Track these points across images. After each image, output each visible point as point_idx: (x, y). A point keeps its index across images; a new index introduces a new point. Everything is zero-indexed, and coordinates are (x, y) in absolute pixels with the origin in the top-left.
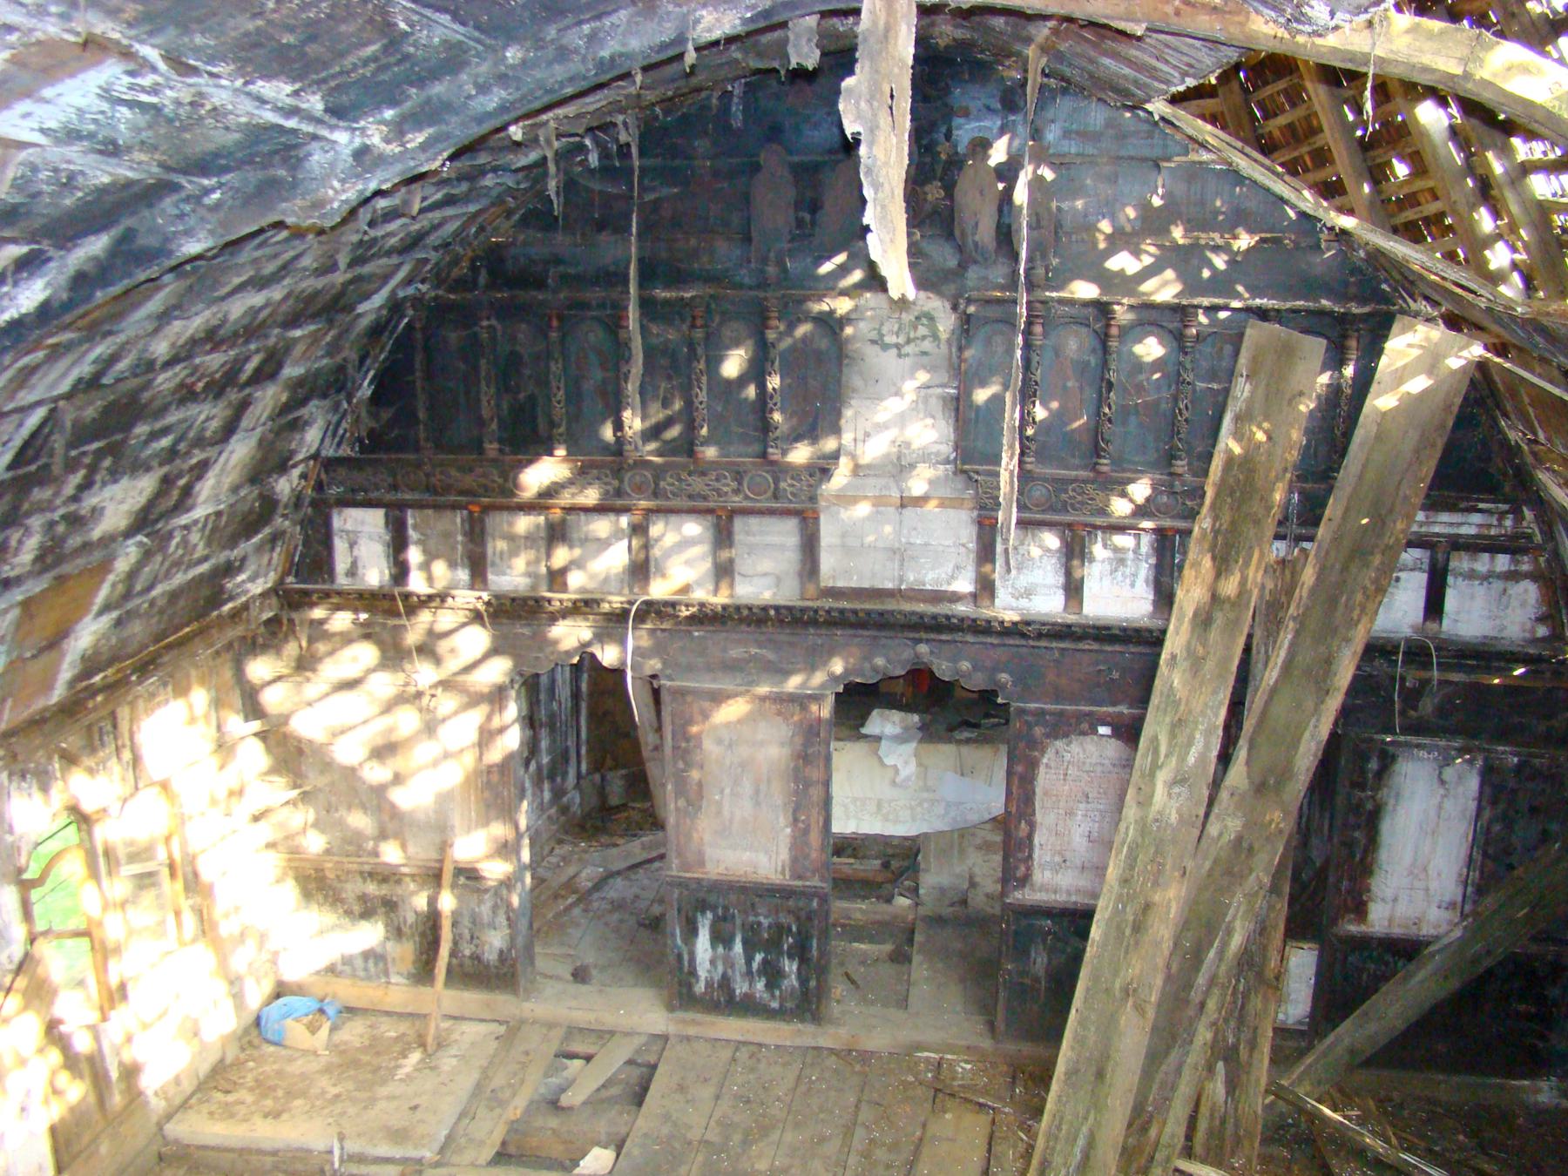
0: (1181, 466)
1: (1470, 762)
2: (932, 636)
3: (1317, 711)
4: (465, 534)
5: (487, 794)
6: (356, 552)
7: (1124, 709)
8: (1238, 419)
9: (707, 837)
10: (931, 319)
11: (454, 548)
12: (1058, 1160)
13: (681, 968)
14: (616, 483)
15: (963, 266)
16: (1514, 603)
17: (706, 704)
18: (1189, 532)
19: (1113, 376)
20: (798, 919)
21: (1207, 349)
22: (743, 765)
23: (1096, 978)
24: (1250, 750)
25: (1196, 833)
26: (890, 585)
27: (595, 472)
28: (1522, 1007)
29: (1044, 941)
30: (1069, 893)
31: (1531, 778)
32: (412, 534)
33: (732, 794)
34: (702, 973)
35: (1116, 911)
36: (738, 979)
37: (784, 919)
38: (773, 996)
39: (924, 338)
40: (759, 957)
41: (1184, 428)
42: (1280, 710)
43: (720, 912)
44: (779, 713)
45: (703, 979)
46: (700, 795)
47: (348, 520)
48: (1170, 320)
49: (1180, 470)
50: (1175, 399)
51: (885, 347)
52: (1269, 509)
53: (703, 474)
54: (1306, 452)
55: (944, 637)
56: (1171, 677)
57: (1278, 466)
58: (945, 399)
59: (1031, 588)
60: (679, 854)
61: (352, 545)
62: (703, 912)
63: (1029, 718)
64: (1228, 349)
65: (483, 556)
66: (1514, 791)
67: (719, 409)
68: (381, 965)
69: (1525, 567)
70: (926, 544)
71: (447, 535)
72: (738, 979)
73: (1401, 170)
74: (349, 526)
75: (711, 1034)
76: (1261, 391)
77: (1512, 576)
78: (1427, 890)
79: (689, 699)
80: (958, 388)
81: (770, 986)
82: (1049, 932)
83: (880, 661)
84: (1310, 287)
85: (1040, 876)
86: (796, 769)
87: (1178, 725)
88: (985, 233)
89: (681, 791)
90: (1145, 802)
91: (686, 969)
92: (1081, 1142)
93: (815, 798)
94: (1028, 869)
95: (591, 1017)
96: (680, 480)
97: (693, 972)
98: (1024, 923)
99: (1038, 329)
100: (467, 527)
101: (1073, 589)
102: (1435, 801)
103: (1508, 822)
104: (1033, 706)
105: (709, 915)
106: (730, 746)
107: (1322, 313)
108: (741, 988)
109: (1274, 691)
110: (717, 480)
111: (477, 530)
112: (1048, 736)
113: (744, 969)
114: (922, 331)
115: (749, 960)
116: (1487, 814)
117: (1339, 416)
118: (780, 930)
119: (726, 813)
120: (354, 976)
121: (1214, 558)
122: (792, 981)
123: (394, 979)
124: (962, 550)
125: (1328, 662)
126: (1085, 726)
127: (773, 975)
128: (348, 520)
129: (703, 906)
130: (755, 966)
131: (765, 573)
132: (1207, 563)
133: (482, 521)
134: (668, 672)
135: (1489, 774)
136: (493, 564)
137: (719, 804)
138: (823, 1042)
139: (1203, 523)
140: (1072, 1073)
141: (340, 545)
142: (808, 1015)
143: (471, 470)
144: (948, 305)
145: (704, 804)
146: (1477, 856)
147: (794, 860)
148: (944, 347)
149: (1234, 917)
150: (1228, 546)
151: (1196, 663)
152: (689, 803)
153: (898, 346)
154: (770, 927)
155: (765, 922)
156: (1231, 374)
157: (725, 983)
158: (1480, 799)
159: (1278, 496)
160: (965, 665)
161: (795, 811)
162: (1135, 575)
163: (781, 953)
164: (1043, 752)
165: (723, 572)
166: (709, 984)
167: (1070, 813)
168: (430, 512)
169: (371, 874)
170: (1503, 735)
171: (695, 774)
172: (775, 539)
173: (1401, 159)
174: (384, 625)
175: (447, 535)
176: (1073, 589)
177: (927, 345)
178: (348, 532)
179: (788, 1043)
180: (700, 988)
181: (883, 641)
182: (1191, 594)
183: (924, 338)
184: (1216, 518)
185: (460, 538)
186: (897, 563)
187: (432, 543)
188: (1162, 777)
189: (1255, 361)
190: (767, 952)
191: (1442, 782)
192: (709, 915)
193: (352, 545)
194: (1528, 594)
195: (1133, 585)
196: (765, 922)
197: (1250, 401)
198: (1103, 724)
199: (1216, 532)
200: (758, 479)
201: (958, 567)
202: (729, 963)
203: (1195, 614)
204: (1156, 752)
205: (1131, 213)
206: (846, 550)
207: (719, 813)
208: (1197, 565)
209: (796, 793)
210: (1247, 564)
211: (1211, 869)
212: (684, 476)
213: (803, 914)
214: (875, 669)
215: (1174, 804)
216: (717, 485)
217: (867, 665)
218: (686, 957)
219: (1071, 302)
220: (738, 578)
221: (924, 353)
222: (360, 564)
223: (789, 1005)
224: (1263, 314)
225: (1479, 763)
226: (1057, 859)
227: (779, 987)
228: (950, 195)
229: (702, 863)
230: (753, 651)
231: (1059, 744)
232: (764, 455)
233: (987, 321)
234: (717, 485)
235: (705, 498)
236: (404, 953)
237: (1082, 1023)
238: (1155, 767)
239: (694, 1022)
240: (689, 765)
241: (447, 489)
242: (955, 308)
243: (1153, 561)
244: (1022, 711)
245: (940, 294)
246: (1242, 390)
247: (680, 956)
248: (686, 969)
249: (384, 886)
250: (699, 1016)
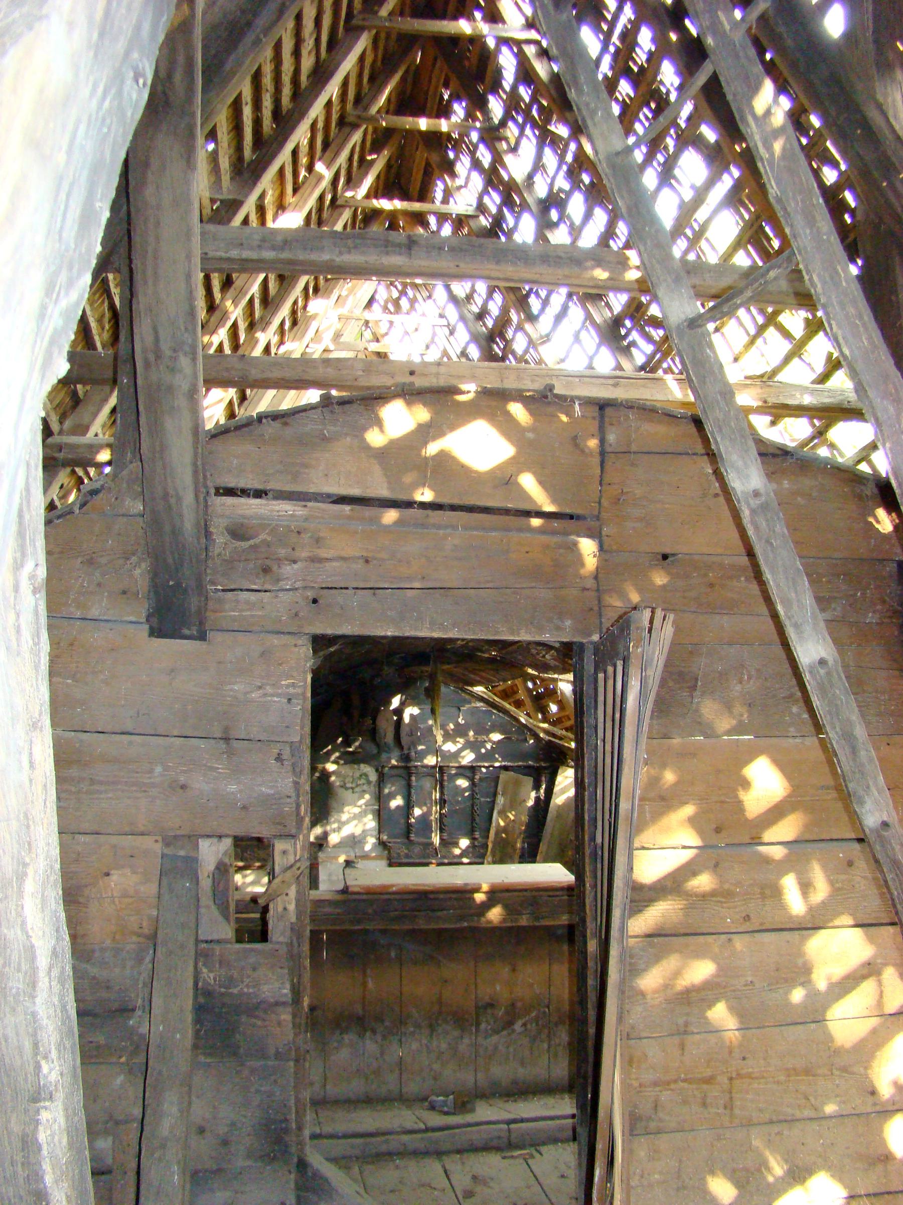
0: (477, 835)
8: (499, 813)
10: (366, 775)
15: (379, 753)
19: (446, 797)
21: (484, 784)
41: (477, 819)
48: (470, 771)
50: (473, 805)
51: (347, 789)
52: (515, 850)
54: (528, 825)
57: (517, 832)
64: (493, 784)
73: (554, 708)
76: (508, 801)
84: (524, 756)
88: (390, 738)
99: (413, 778)
107: (529, 767)
117: (542, 807)
148: (372, 788)
156: (495, 795)
159: (519, 845)
173: (554, 703)
189: (504, 788)
197: (504, 805)
205: (452, 726)
219: (427, 766)
224: (506, 768)
228: (374, 722)
233: (392, 776)
242: (377, 770)
245: (370, 765)
246: (500, 800)
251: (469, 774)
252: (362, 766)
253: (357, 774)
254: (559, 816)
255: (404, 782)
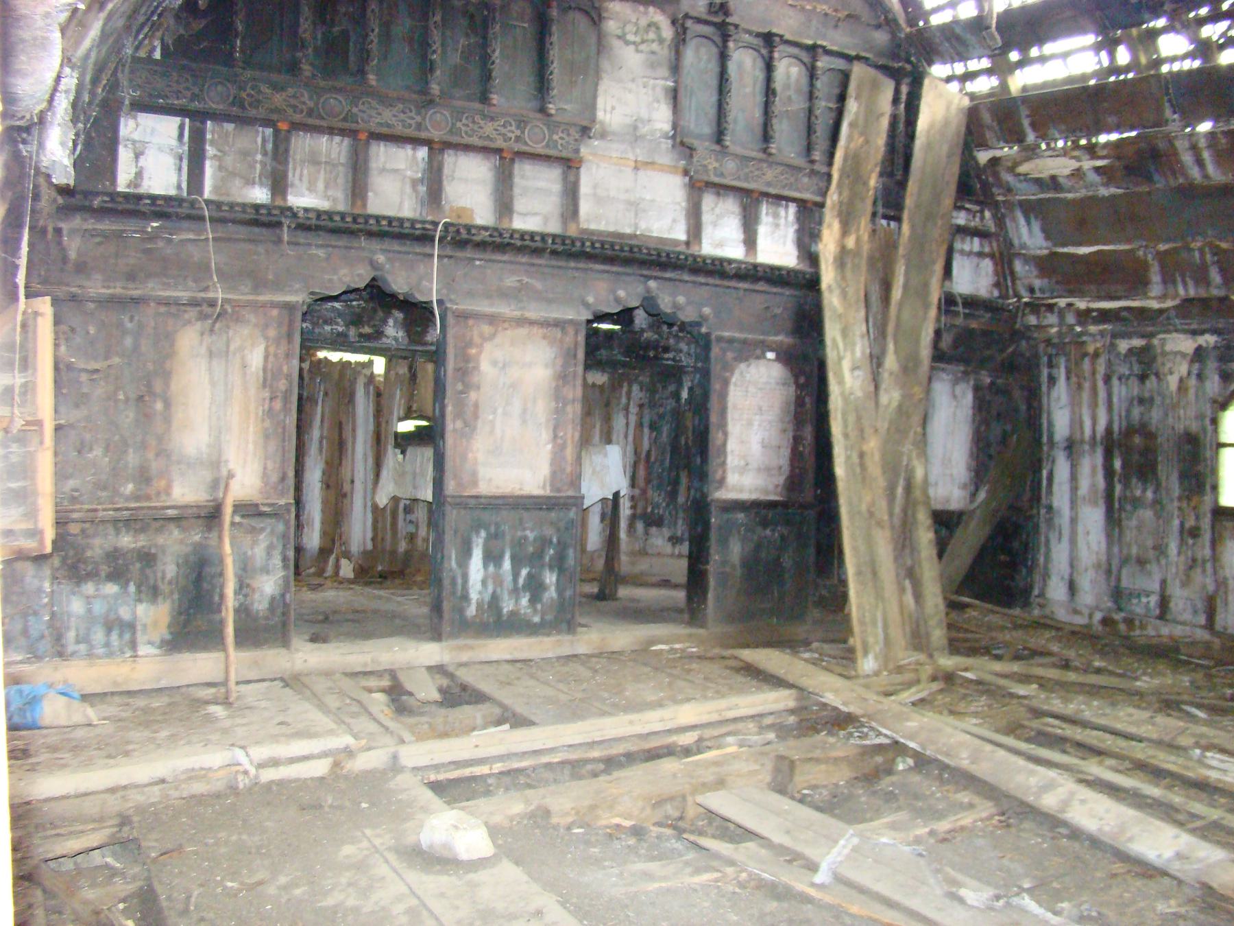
1: (968, 382)
2: (659, 274)
3: (925, 318)
4: (265, 154)
5: (267, 423)
6: (142, 162)
7: (780, 338)
8: (851, 125)
9: (481, 457)
10: (658, 28)
11: (252, 167)
12: (871, 640)
13: (454, 593)
14: (419, 119)
16: (983, 273)
17: (486, 329)
18: (821, 205)
20: (558, 530)
22: (513, 386)
23: (850, 504)
24: (896, 343)
25: (873, 405)
26: (628, 231)
27: (401, 106)
28: (1002, 557)
29: (739, 532)
30: (750, 492)
31: (996, 393)
32: (210, 150)
33: (505, 414)
34: (474, 596)
35: (848, 458)
36: (506, 596)
37: (549, 532)
38: (535, 610)
39: (653, 41)
40: (524, 572)
42: (906, 315)
43: (493, 529)
44: (544, 337)
45: (474, 602)
46: (476, 416)
47: (134, 127)
49: (817, 158)
51: (627, 43)
53: (492, 119)
55: (668, 275)
56: (832, 300)
58: (666, 90)
59: (723, 238)
60: (455, 477)
61: (138, 155)
62: (478, 533)
63: (724, 345)
65: (284, 176)
66: (989, 402)
67: (506, 68)
68: (127, 636)
69: (987, 250)
70: (653, 201)
71: (245, 154)
72: (506, 596)
74: (136, 136)
75: (483, 656)
76: (862, 109)
77: (981, 255)
78: (951, 475)
79: (471, 322)
80: (675, 82)
81: (534, 600)
82: (742, 525)
83: (621, 293)
85: (732, 478)
86: (557, 389)
87: (845, 332)
89: (459, 415)
90: (841, 382)
91: (459, 594)
92: (880, 624)
93: (570, 416)
94: (724, 472)
95: (367, 658)
96: (474, 122)
97: (465, 597)
98: (726, 516)
100: (270, 146)
101: (750, 242)
102: (952, 410)
103: (988, 425)
104: (726, 334)
105: (483, 534)
106: (504, 366)
108: (508, 606)
109: (901, 304)
110: (504, 126)
111: (281, 149)
112: (735, 359)
113: (511, 586)
114: (652, 36)
115: (516, 575)
116: (978, 418)
118: (544, 542)
119: (498, 431)
120: (90, 655)
121: (841, 222)
122: (551, 593)
123: (143, 650)
124: (678, 207)
125: (926, 285)
126: (758, 352)
127: (535, 587)
128: (134, 127)
129: (477, 526)
130: (521, 581)
131: (536, 211)
132: (836, 225)
133: (287, 140)
134: (453, 297)
135: (977, 389)
136: (292, 185)
137: (492, 423)
138: (582, 649)
139: (833, 198)
140: (859, 573)
141: (124, 154)
142: (564, 626)
143: (283, 89)
144: (669, 22)
145: (480, 424)
146: (975, 450)
147: (554, 474)
149: (910, 460)
150: (849, 214)
151: (844, 294)
152: (466, 424)
153: (634, 43)
154: (535, 540)
155: (531, 535)
157: (495, 600)
158: (973, 408)
160: (681, 299)
161: (556, 428)
162: (785, 236)
163: (543, 566)
164: (732, 374)
165: (504, 205)
166: (480, 605)
167: (750, 423)
168: (230, 127)
169: (127, 522)
170: (982, 363)
171: (473, 395)
172: (541, 184)
174: (170, 241)
175: (245, 154)
176: (750, 242)
177: (655, 46)
178: (134, 142)
179: (550, 655)
180: (471, 611)
181: (624, 278)
182: (828, 244)
183: (653, 41)
184: (840, 194)
185: (259, 157)
186: (632, 214)
187: (229, 160)
188: (846, 365)
189: (859, 87)
190: (532, 567)
191: (954, 396)
192: (483, 534)
193: (138, 155)
194: (987, 265)
195: (784, 244)
196: (531, 535)
197: (857, 114)
198: (772, 350)
199: (841, 203)
200: (537, 130)
201: (674, 221)
202: (498, 581)
203: (835, 259)
204: (838, 348)
206: (599, 200)
207: (492, 432)
208: (830, 226)
209: (557, 411)
210: (858, 229)
211: (888, 429)
212: (477, 118)
213: (562, 525)
214: (618, 300)
215: (858, 383)
216: (503, 130)
217: (611, 298)
218: (460, 581)
220: (515, 216)
221: (653, 53)
222: (146, 175)
223: (549, 617)
225: (972, 383)
226: (743, 463)
227: (540, 600)
229: (475, 483)
230: (526, 280)
231: (743, 366)
232: (543, 110)
234: (503, 130)
235: (491, 140)
236: (154, 616)
237: (853, 537)
238: (840, 359)
239: (471, 648)
240: (468, 387)
241: (256, 103)
242: (674, 22)
243: (796, 227)
244: (720, 339)
245: (663, 11)
247: (454, 580)
248: (459, 594)
249: (142, 537)
250: (470, 642)
251: (806, 59)
252: (651, 9)
253: (643, 22)
254: (929, 146)
255: (715, 50)
